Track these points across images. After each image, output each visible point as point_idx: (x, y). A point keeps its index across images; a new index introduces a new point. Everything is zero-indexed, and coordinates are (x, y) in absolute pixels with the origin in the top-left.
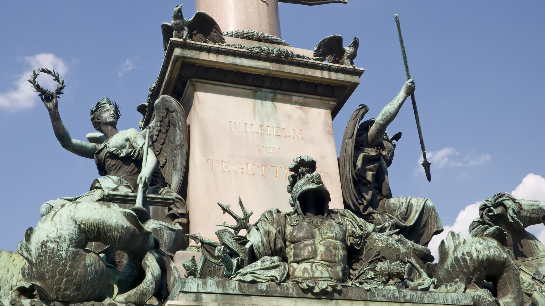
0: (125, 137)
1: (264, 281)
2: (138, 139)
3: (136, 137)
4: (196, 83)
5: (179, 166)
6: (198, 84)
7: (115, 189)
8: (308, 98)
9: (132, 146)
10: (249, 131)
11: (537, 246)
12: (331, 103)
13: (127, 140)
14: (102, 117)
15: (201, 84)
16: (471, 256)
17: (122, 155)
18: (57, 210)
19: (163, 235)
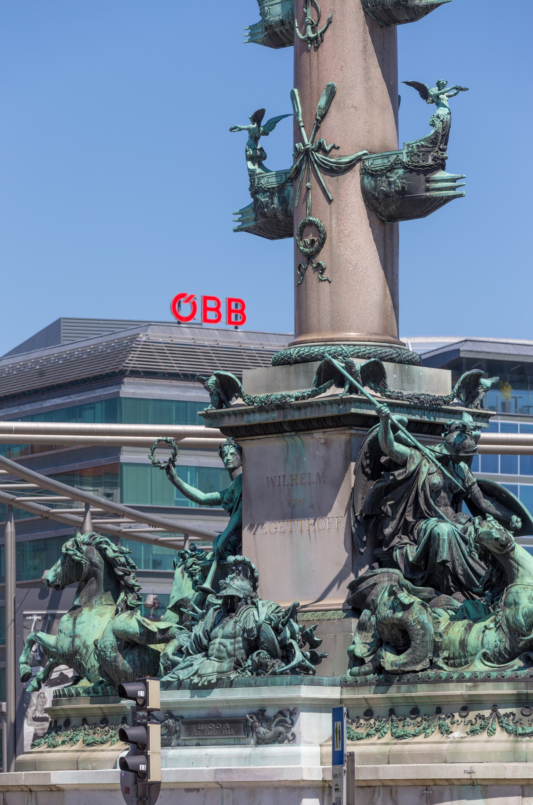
1: (175, 680)
10: (282, 483)
11: (518, 570)
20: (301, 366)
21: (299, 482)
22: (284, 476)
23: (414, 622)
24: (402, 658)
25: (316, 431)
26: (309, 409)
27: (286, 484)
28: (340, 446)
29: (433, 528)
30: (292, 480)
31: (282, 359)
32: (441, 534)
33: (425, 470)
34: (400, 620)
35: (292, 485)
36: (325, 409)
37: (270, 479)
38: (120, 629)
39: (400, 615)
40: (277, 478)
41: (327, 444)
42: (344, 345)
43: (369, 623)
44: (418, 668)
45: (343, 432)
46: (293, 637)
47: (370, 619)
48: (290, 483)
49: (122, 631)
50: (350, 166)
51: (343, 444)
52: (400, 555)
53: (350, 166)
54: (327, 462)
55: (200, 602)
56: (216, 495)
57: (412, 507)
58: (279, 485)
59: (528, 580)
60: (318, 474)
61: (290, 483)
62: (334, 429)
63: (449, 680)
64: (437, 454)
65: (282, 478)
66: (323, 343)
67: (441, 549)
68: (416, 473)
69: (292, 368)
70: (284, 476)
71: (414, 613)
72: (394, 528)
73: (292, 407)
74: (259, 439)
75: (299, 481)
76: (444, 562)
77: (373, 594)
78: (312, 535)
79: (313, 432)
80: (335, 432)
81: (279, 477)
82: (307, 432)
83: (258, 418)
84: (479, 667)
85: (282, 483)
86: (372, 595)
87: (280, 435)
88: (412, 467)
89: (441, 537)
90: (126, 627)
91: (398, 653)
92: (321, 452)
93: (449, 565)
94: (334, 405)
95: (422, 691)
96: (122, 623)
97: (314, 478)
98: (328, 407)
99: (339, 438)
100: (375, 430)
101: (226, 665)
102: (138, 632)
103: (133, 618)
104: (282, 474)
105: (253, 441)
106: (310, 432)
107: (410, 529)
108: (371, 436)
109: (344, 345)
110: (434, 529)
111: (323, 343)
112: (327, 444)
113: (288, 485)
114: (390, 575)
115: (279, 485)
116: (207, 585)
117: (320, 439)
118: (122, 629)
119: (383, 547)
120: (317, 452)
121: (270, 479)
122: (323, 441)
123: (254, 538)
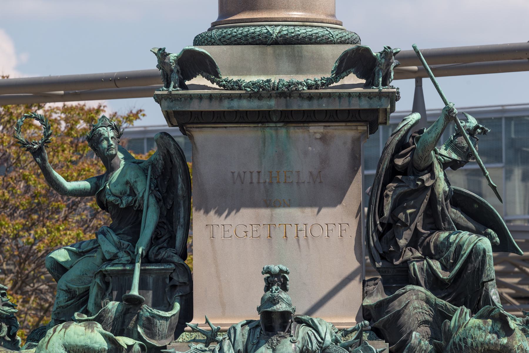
0: (125, 180)
2: (139, 183)
3: (136, 182)
4: (191, 129)
5: (182, 220)
6: (195, 130)
7: (115, 256)
8: (329, 126)
9: (133, 193)
10: (255, 180)
12: (359, 128)
13: (127, 183)
14: (99, 148)
15: (197, 130)
16: (466, 343)
17: (121, 206)
18: (50, 335)
19: (156, 324)
20: (284, 49)
21: (282, 179)
22: (259, 172)
23: (518, 349)
25: (313, 125)
26: (325, 100)
27: (262, 181)
28: (345, 143)
29: (477, 243)
30: (271, 177)
31: (253, 38)
32: (487, 250)
34: (504, 347)
35: (271, 183)
36: (349, 102)
37: (236, 174)
38: (79, 344)
39: (504, 341)
40: (248, 175)
41: (324, 139)
42: (270, 26)
43: (418, 347)
45: (354, 128)
47: (420, 342)
48: (267, 180)
49: (82, 346)
51: (349, 142)
52: (419, 271)
54: (324, 161)
55: (121, 313)
56: (84, 184)
57: (422, 217)
58: (251, 183)
60: (311, 173)
61: (267, 180)
62: (344, 124)
64: (446, 158)
65: (255, 175)
66: (301, 23)
67: (488, 266)
69: (270, 49)
70: (259, 172)
71: (517, 339)
72: (409, 239)
73: (301, 96)
74: (225, 127)
75: (282, 179)
77: (406, 314)
78: (302, 242)
79: (310, 125)
80: (343, 127)
81: (251, 173)
82: (302, 125)
83: (245, 105)
85: (255, 180)
86: (405, 315)
87: (260, 125)
89: (487, 253)
90: (89, 342)
92: (317, 148)
94: (363, 98)
96: (82, 337)
97: (305, 177)
98: (354, 99)
99: (343, 135)
100: (403, 129)
102: (107, 348)
103: (96, 332)
104: (255, 169)
105: (215, 130)
106: (306, 125)
107: (420, 241)
108: (400, 135)
109: (270, 26)
110: (477, 244)
111: (301, 23)
112: (324, 139)
113: (265, 182)
114: (417, 293)
115: (251, 183)
116: (135, 292)
117: (315, 133)
118: (83, 343)
119: (394, 260)
120: (310, 148)
121: (236, 174)
122: (318, 136)
123: (212, 241)
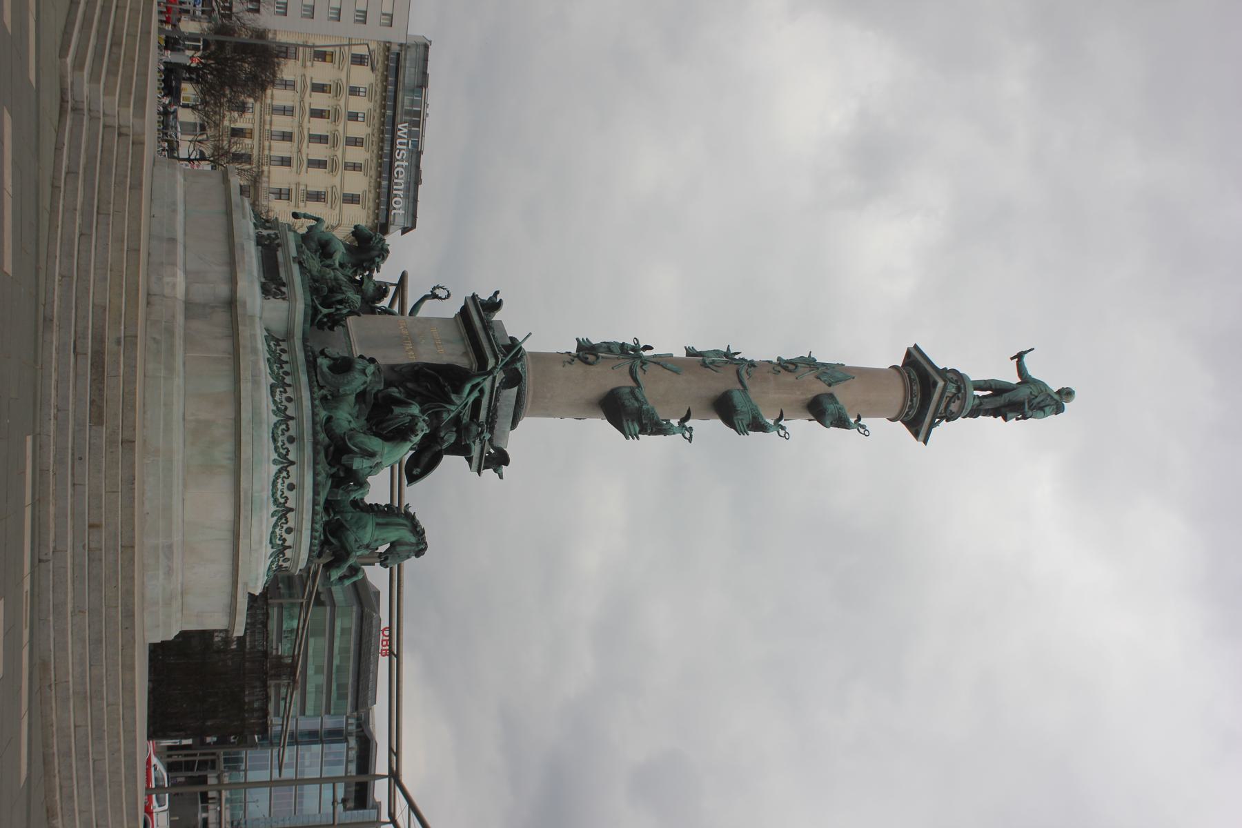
24: (325, 369)
33: (453, 408)
44: (319, 377)
46: (338, 309)
50: (635, 380)
53: (635, 380)
59: (386, 450)
63: (312, 392)
68: (451, 402)
76: (392, 411)
84: (323, 414)
88: (453, 397)
91: (330, 368)
93: (390, 416)
95: (304, 379)
101: (315, 273)
